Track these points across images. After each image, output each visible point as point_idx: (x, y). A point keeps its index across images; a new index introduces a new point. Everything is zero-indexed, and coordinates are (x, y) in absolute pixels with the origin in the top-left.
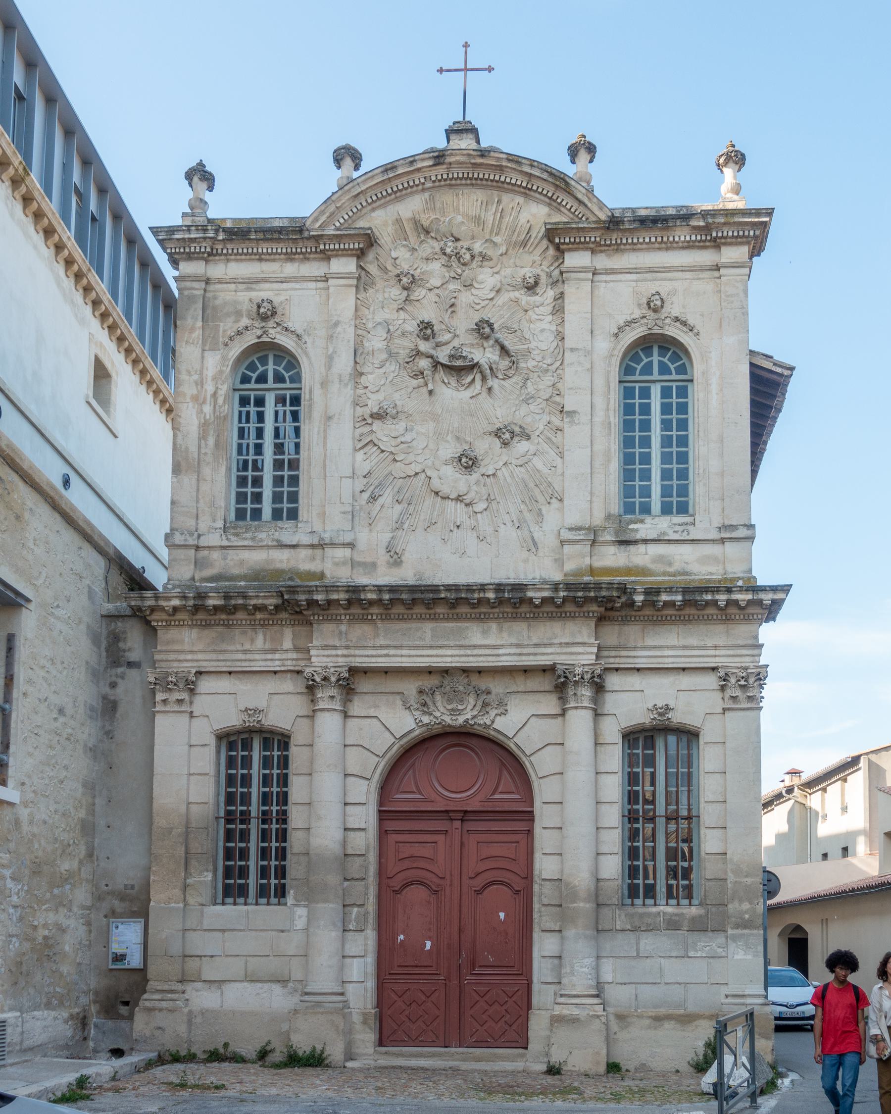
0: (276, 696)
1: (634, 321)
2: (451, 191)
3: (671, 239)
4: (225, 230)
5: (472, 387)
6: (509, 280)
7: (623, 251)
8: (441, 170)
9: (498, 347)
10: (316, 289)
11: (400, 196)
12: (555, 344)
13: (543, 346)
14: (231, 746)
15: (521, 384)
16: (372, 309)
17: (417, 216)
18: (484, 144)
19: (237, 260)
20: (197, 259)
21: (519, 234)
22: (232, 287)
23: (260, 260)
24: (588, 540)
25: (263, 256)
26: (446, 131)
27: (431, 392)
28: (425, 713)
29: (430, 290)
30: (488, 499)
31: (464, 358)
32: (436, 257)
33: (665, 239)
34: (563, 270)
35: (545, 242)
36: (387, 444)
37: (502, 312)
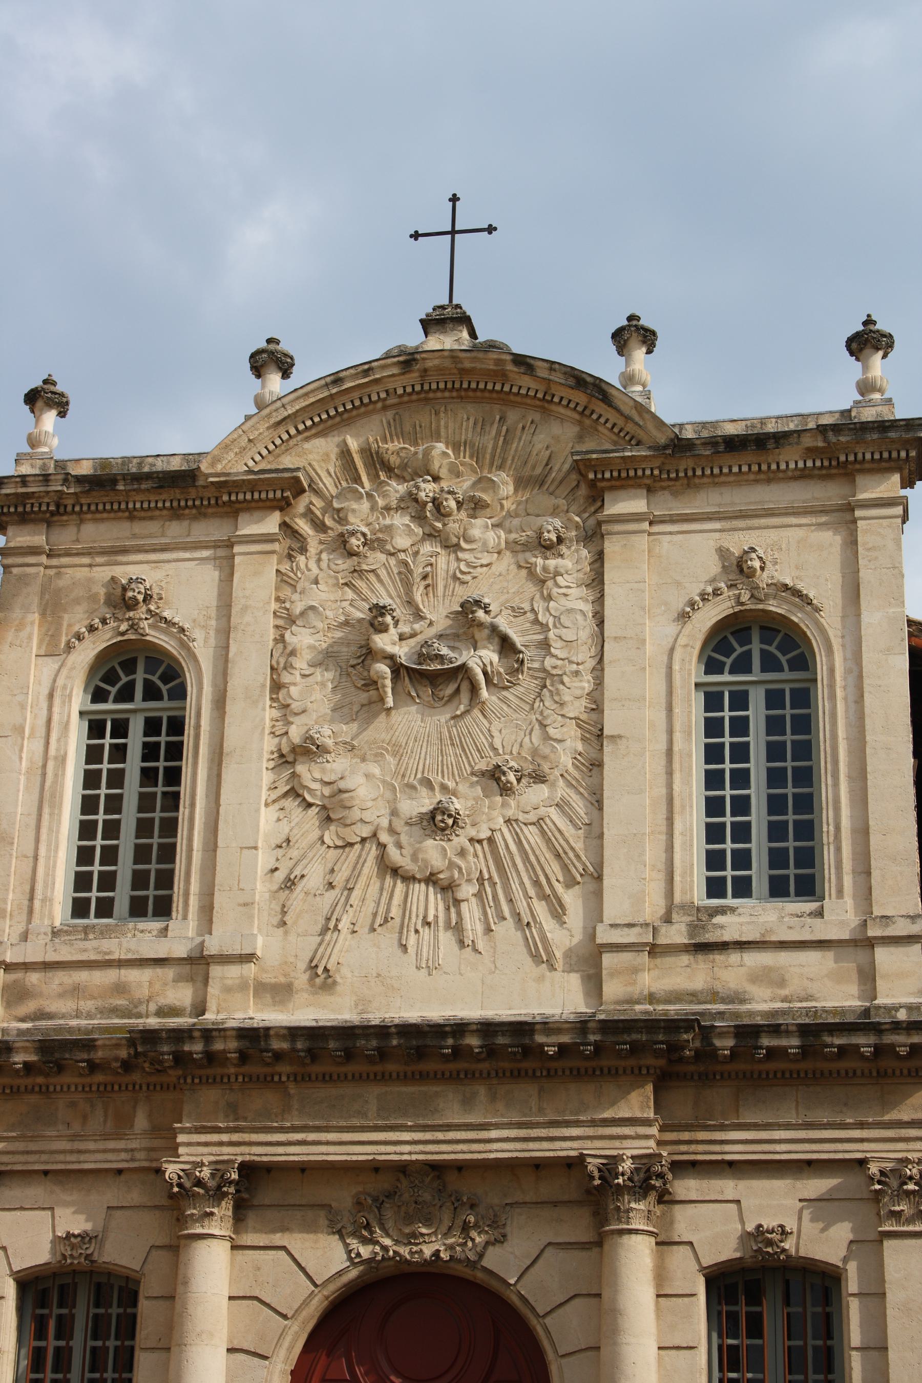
0: (118, 1213)
3: (774, 467)
4: (80, 480)
5: (455, 702)
8: (413, 377)
10: (215, 559)
11: (348, 419)
13: (569, 635)
14: (42, 1301)
18: (482, 337)
19: (95, 520)
20: (33, 521)
21: (534, 468)
22: (86, 560)
23: (131, 518)
24: (646, 944)
25: (136, 513)
26: (421, 321)
28: (365, 1241)
30: (481, 880)
31: (440, 658)
33: (764, 467)
35: (574, 476)
36: (316, 791)
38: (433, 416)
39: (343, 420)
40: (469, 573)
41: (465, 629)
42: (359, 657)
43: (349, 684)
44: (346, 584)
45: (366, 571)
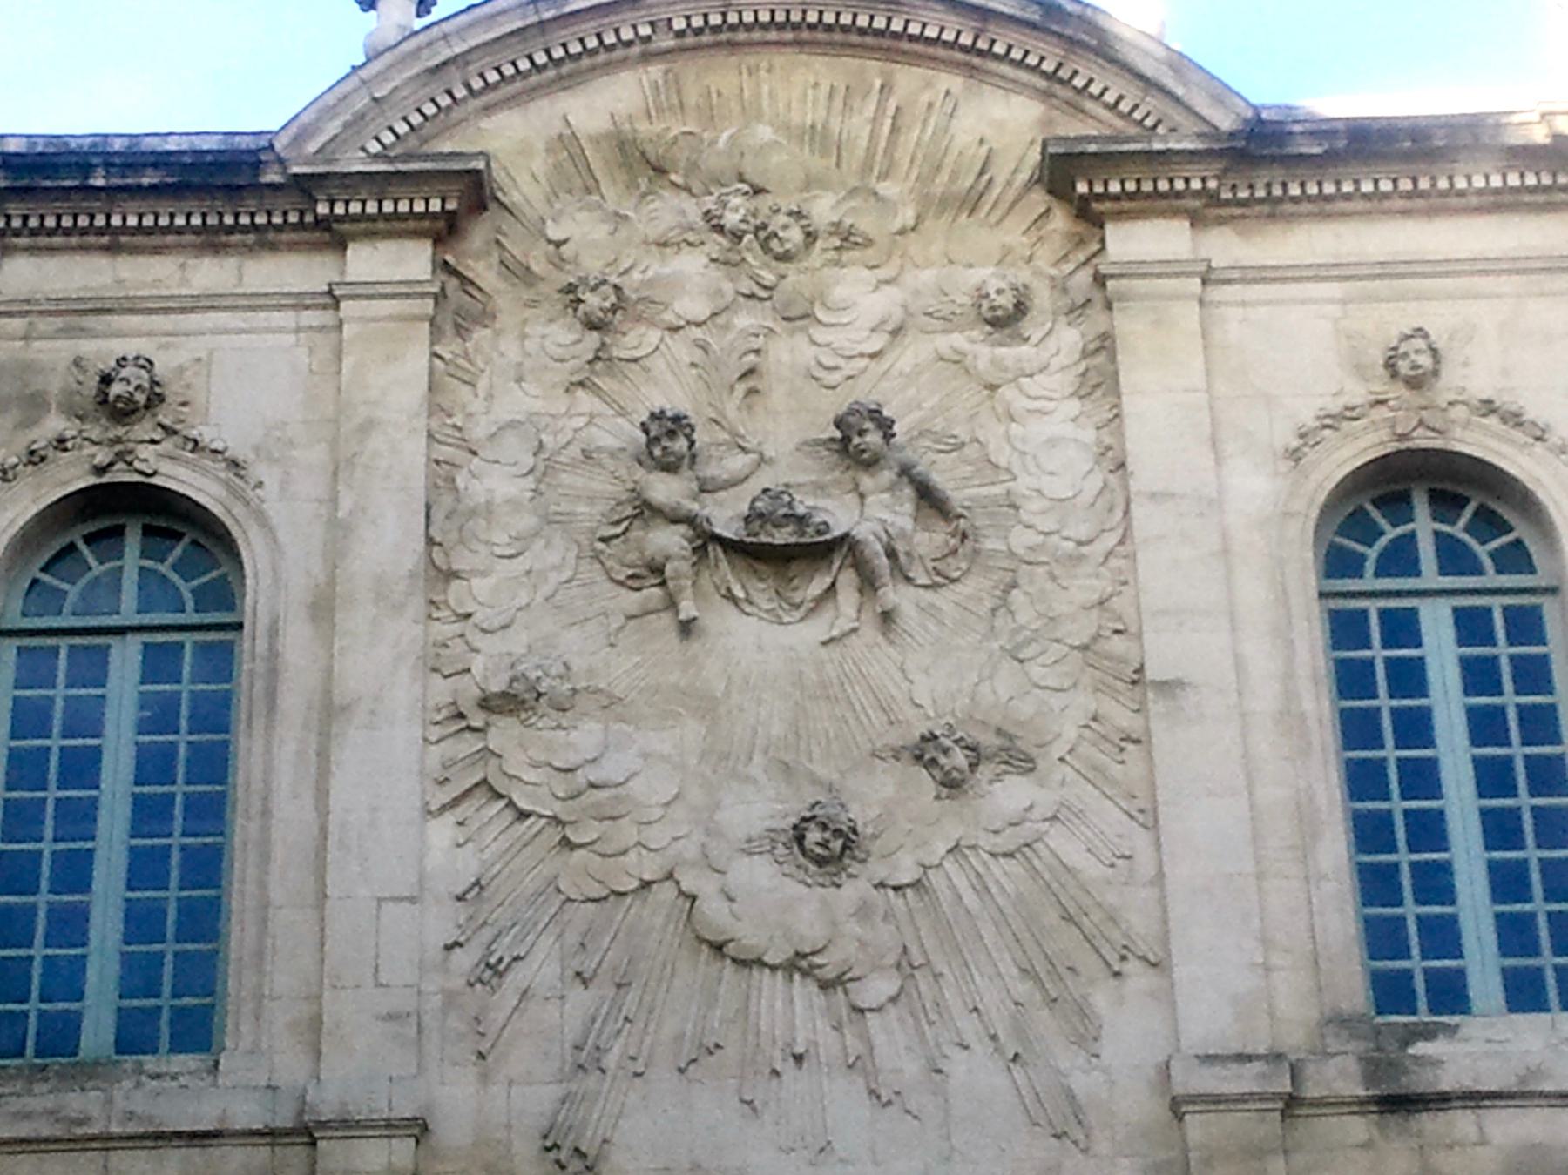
1: (1349, 414)
2: (733, 59)
5: (827, 614)
6: (932, 303)
7: (1290, 218)
9: (908, 491)
10: (298, 330)
12: (1096, 482)
13: (1059, 488)
15: (988, 604)
16: (482, 384)
17: (627, 127)
23: (113, 249)
25: (123, 239)
27: (687, 628)
29: (675, 329)
31: (801, 521)
32: (691, 237)
34: (1104, 270)
35: (1039, 199)
37: (911, 392)
38: (745, 76)
39: (561, 78)
40: (836, 368)
41: (837, 473)
42: (618, 523)
43: (600, 578)
44: (581, 384)
45: (621, 360)
